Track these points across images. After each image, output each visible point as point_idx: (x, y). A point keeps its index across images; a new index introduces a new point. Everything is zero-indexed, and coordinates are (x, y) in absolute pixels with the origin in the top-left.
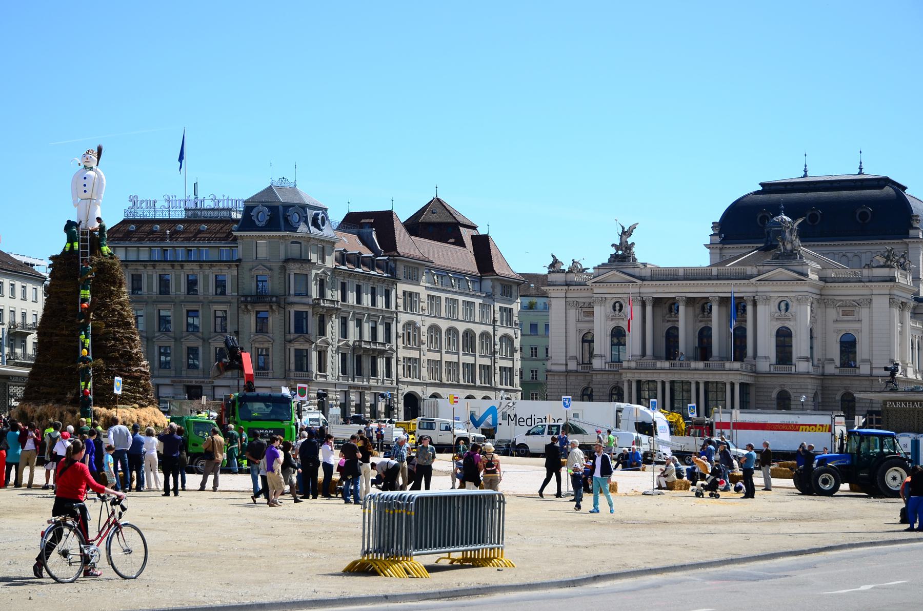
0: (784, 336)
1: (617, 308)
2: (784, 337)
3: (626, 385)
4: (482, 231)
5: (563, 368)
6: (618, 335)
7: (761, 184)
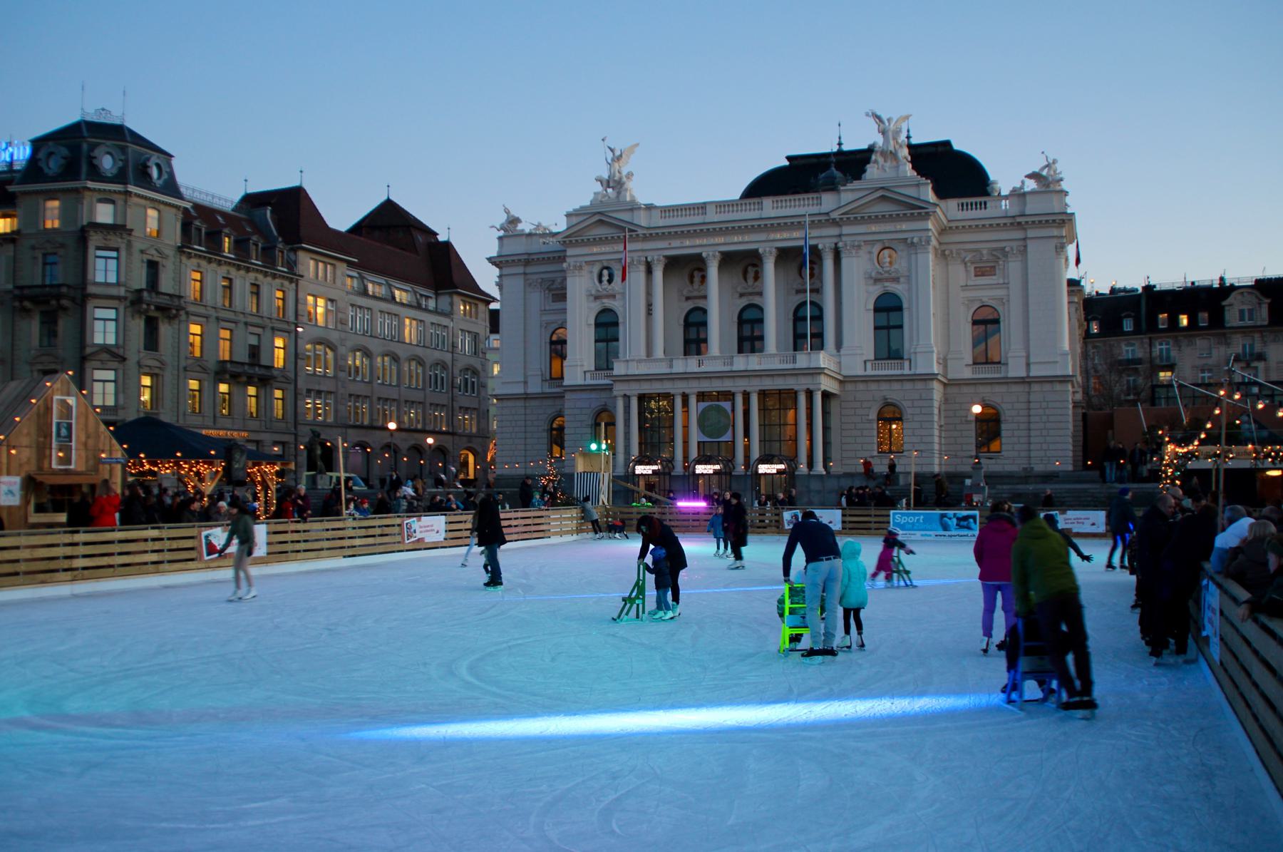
0: (888, 310)
1: (605, 278)
2: (889, 311)
3: (620, 404)
4: (441, 238)
5: (519, 390)
6: (607, 326)
7: (789, 158)
